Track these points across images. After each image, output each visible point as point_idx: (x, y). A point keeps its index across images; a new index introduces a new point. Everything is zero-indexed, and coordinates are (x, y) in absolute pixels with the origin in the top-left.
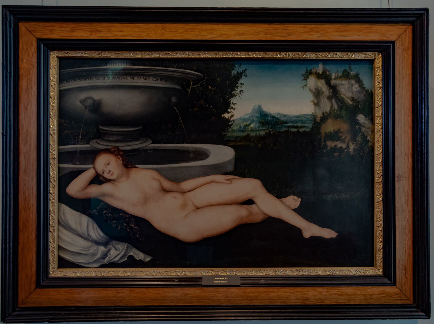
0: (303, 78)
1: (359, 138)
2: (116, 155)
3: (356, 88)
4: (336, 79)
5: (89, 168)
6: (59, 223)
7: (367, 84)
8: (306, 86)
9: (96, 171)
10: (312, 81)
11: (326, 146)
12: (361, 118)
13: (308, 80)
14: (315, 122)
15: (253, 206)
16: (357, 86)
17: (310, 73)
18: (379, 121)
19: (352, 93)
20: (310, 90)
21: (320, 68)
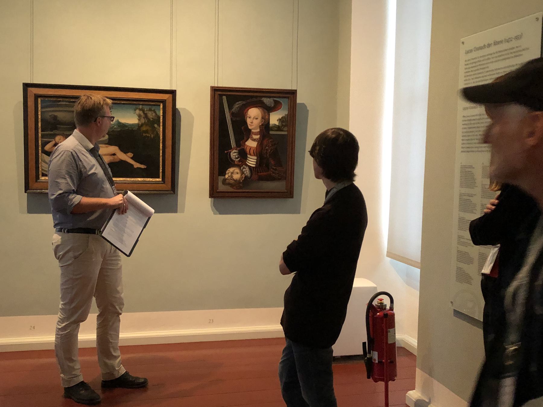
0: (134, 110)
1: (155, 133)
2: (63, 136)
3: (154, 114)
4: (146, 111)
5: (53, 141)
6: (42, 160)
7: (157, 112)
8: (135, 113)
9: (56, 142)
10: (138, 112)
11: (143, 135)
12: (156, 126)
13: (136, 111)
14: (139, 126)
15: (115, 156)
16: (154, 114)
17: (137, 108)
18: (161, 127)
19: (153, 116)
20: (137, 115)
21: (141, 106)
